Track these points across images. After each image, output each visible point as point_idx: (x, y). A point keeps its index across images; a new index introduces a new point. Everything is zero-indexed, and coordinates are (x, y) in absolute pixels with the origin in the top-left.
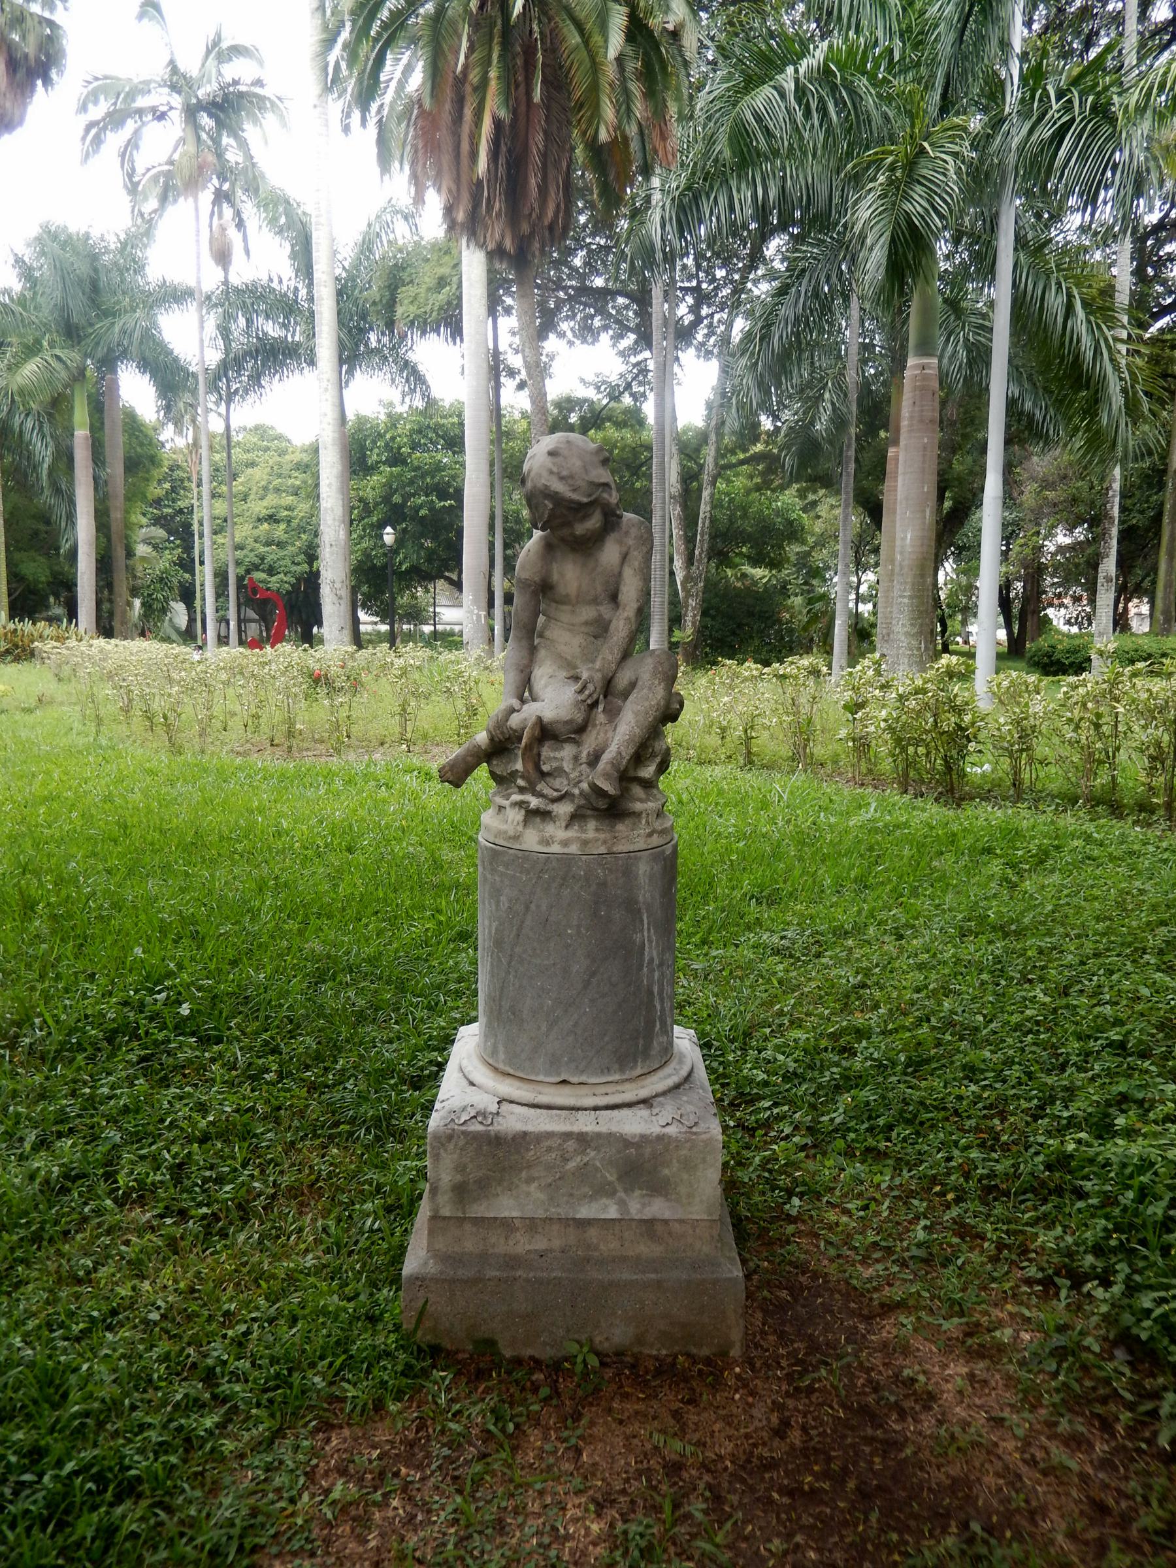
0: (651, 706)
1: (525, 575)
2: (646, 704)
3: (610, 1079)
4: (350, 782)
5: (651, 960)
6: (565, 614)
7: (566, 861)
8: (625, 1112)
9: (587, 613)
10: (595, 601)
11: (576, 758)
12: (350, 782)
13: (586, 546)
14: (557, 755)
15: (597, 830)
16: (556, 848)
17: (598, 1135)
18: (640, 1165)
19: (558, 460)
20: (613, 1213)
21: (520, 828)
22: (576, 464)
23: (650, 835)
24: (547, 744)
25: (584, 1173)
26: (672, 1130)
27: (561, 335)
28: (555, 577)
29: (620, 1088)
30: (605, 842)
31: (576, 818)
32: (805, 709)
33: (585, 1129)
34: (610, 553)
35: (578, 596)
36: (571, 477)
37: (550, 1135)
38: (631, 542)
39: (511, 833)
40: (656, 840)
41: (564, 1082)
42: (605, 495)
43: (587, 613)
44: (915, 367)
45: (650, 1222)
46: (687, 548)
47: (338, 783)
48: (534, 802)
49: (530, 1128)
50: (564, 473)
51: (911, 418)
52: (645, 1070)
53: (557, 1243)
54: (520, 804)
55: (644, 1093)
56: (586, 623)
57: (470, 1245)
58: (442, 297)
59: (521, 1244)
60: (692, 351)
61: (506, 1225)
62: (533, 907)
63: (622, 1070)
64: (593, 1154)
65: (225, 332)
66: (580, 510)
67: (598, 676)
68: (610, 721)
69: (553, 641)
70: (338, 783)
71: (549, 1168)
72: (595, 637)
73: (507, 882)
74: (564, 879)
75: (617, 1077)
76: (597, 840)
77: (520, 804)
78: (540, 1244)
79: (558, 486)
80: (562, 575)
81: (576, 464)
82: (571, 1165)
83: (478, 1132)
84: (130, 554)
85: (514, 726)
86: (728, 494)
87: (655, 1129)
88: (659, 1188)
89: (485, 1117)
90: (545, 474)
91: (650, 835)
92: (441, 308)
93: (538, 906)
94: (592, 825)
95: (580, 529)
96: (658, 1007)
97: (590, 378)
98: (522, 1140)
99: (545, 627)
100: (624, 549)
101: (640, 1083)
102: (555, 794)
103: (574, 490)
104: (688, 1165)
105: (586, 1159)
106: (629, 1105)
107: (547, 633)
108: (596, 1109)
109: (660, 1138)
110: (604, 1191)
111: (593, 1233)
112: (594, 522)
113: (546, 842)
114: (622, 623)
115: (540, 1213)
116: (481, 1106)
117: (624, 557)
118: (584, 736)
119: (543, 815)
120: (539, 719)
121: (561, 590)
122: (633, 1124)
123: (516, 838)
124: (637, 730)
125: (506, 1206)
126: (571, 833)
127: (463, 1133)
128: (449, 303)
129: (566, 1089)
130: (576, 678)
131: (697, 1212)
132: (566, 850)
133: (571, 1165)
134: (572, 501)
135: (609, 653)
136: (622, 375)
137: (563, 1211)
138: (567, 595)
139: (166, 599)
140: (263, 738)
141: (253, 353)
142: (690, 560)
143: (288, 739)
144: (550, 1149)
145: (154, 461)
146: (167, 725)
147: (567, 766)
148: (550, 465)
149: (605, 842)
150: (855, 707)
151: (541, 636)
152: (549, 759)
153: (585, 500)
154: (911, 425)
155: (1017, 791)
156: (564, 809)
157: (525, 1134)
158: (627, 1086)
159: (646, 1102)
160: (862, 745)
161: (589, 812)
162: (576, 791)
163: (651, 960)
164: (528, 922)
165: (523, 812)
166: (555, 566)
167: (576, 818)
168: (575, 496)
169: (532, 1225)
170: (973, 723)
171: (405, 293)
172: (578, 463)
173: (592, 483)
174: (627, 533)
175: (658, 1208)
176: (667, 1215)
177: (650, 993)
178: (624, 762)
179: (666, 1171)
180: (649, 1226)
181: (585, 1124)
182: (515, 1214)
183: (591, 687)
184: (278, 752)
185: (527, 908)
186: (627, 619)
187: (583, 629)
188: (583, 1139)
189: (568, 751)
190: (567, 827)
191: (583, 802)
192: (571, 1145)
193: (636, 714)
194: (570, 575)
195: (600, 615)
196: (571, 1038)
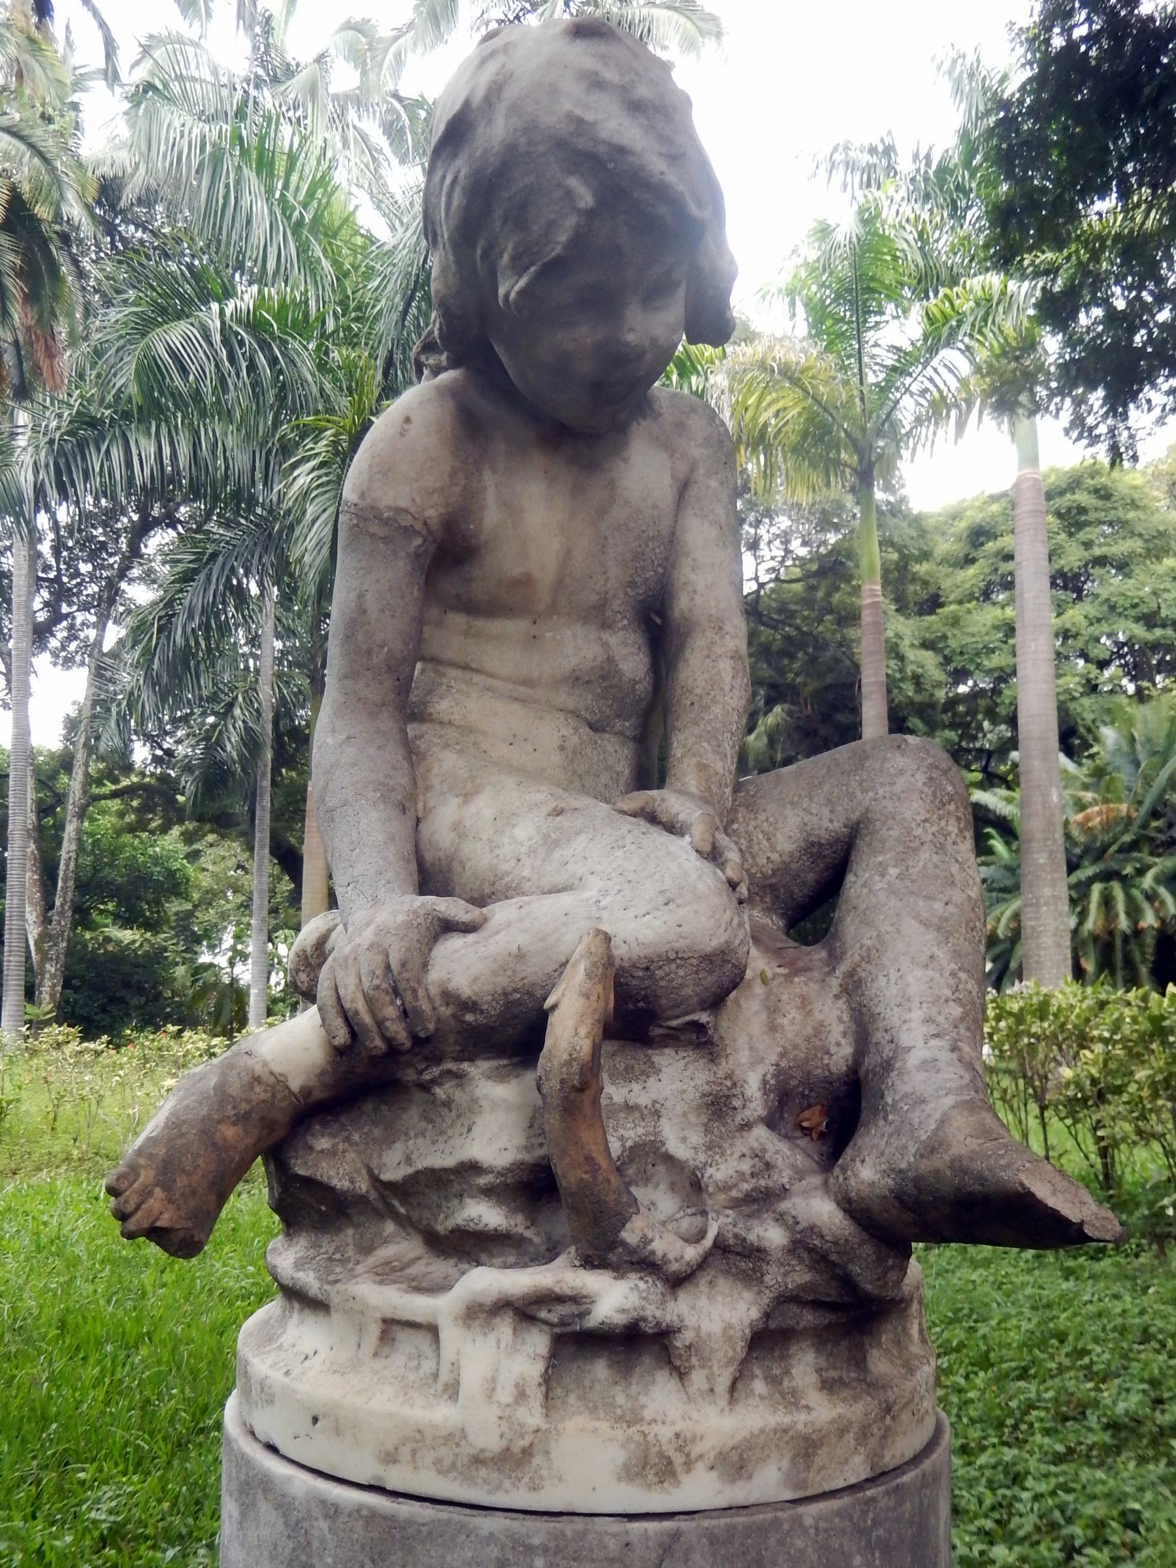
1: (395, 496)
28: (491, 516)
48: (613, 1298)
77: (524, 1311)
80: (512, 509)
85: (463, 985)
94: (804, 1367)
119: (638, 1344)
126: (756, 1416)
132: (740, 1493)
156: (719, 1314)
162: (773, 1236)
191: (800, 1276)
194: (532, 518)
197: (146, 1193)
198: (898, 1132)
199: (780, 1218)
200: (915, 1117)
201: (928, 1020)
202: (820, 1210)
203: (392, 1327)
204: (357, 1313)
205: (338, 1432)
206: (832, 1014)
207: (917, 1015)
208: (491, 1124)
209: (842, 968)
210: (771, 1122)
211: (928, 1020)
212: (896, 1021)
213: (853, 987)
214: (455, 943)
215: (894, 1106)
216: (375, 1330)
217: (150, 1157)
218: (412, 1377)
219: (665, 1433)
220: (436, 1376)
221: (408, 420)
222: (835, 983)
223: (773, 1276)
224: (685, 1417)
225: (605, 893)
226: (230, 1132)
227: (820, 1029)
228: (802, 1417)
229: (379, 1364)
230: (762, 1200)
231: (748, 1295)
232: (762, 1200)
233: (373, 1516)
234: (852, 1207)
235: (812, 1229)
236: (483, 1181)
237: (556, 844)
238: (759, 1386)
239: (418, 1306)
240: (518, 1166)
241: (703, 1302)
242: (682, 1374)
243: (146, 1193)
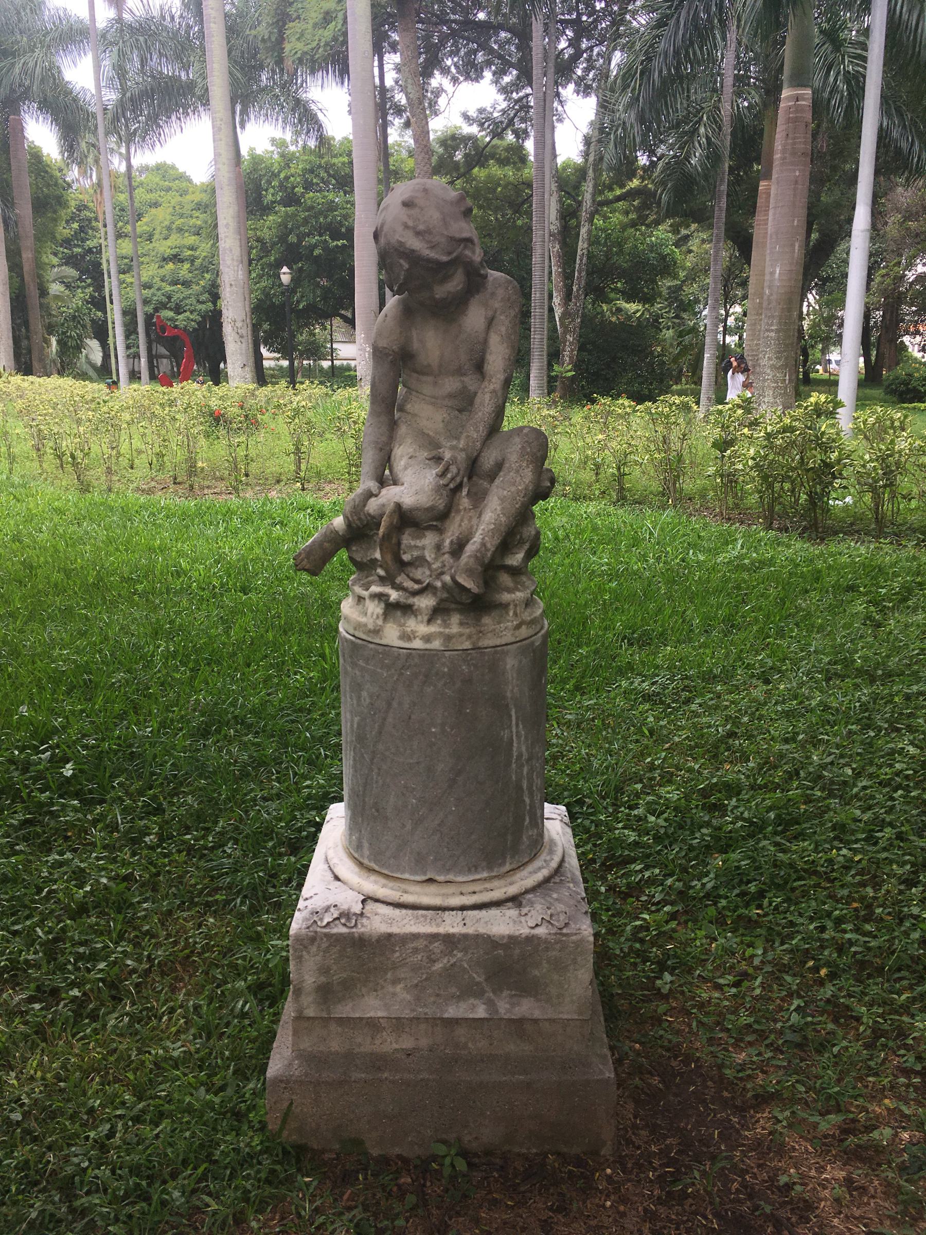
0: (518, 491)
2: (513, 489)
3: (477, 877)
4: (247, 520)
5: (520, 756)
7: (427, 656)
8: (494, 912)
9: (450, 385)
10: (459, 372)
11: (438, 547)
12: (247, 520)
13: (448, 311)
14: (419, 543)
15: (461, 624)
16: (417, 644)
17: (465, 936)
18: (508, 965)
19: (414, 212)
20: (481, 1012)
21: (380, 622)
22: (433, 216)
23: (518, 627)
24: (408, 531)
25: (450, 974)
26: (541, 931)
27: (445, 71)
28: (416, 345)
29: (488, 885)
30: (469, 637)
31: (437, 612)
32: (675, 445)
33: (452, 931)
34: (474, 318)
35: (440, 366)
36: (428, 231)
37: (416, 936)
38: (497, 305)
40: (524, 632)
41: (431, 881)
42: (468, 253)
43: (450, 385)
44: (789, 98)
45: (521, 1021)
46: (565, 285)
47: (236, 522)
48: (394, 595)
49: (395, 930)
50: (421, 227)
51: (784, 151)
52: (514, 866)
53: (424, 1042)
54: (379, 597)
55: (512, 890)
56: (451, 396)
57: (335, 1045)
58: (327, 34)
59: (389, 1044)
60: (571, 87)
61: (373, 1025)
62: (395, 704)
63: (490, 868)
64: (459, 955)
65: (120, 71)
66: (440, 270)
67: (461, 456)
68: (475, 507)
70: (236, 522)
71: (416, 969)
72: (460, 411)
73: (367, 677)
74: (426, 676)
75: (485, 875)
76: (461, 635)
77: (379, 597)
78: (407, 1043)
79: (415, 244)
81: (433, 216)
82: (438, 966)
83: (341, 934)
84: (43, 292)
85: (371, 512)
86: (604, 230)
87: (525, 931)
88: (527, 987)
89: (349, 919)
90: (400, 229)
91: (518, 627)
92: (327, 44)
93: (400, 704)
94: (455, 619)
95: (443, 290)
96: (527, 800)
97: (473, 113)
98: (388, 942)
99: (406, 400)
100: (490, 313)
101: (509, 880)
102: (416, 587)
103: (432, 248)
104: (559, 966)
105: (453, 960)
106: (497, 904)
107: (408, 407)
108: (463, 908)
109: (530, 939)
110: (470, 991)
111: (461, 1032)
112: (456, 284)
114: (487, 396)
115: (407, 1014)
116: (345, 907)
117: (490, 322)
118: (448, 523)
120: (398, 506)
122: (501, 924)
123: (377, 631)
124: (503, 519)
125: (372, 1007)
126: (433, 629)
127: (326, 935)
128: (335, 39)
129: (432, 888)
130: (438, 459)
131: (568, 1012)
132: (428, 646)
133: (438, 966)
134: (429, 260)
135: (475, 432)
136: (504, 112)
137: (430, 1011)
138: (429, 366)
139: (80, 337)
140: (166, 476)
141: (147, 94)
142: (568, 296)
143: (189, 477)
144: (416, 951)
145: (61, 202)
146: (75, 464)
147: (429, 556)
148: (405, 218)
149: (469, 637)
150: (723, 445)
151: (401, 409)
152: (411, 547)
153: (445, 258)
154: (784, 158)
155: (879, 526)
156: (425, 603)
157: (390, 936)
158: (496, 883)
159: (515, 900)
160: (730, 480)
161: (453, 606)
162: (439, 584)
163: (520, 756)
164: (390, 720)
165: (383, 605)
167: (437, 612)
168: (433, 255)
169: (398, 1025)
170: (839, 461)
171: (293, 28)
172: (436, 215)
173: (452, 239)
174: (493, 294)
175: (527, 1008)
176: (537, 1014)
177: (519, 788)
178: (489, 554)
179: (537, 973)
180: (519, 1026)
181: (451, 925)
182: (380, 1014)
183: (453, 469)
184: (181, 490)
185: (389, 704)
186: (494, 391)
188: (449, 940)
189: (429, 540)
190: (429, 621)
191: (445, 595)
192: (437, 946)
193: (502, 500)
194: (431, 343)
195: (465, 387)
196: (436, 837)
197: (302, 560)
219: (409, 629)
223: (439, 594)
226: (327, 545)
228: (447, 631)
233: (352, 642)
238: (439, 622)
242: (416, 616)
243: (302, 560)
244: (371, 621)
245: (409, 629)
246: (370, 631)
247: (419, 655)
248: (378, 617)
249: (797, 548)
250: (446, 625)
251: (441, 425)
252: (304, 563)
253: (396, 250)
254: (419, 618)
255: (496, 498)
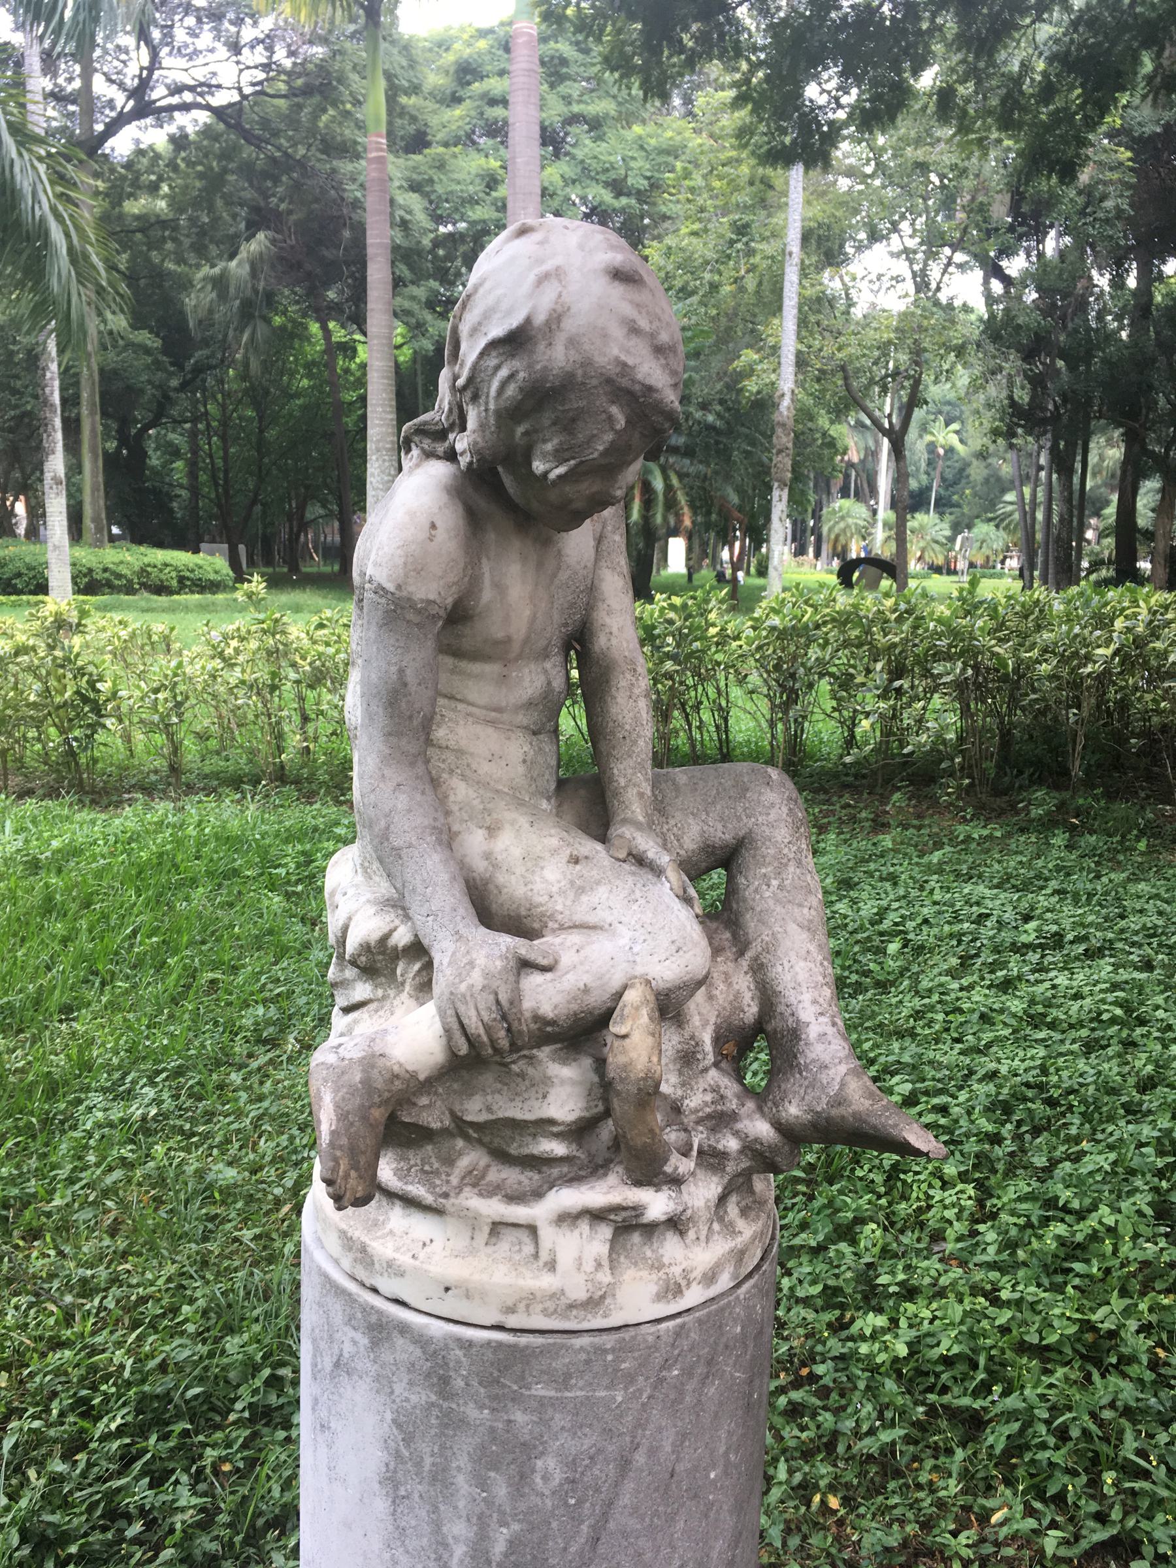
6: (479, 685)
16: (694, 1296)
35: (527, 640)
39: (579, 1293)
54: (597, 1216)
56: (530, 704)
69: (459, 752)
72: (535, 733)
80: (500, 588)
90: (617, 332)
93: (653, 1452)
113: (673, 1290)
121: (493, 627)
126: (720, 1247)
138: (508, 640)
148: (628, 311)
155: (175, 780)
156: (703, 1191)
162: (732, 1144)
165: (606, 1231)
166: (486, 567)
185: (625, 1464)
187: (522, 719)
193: (808, 928)
197: (347, 1176)
198: (812, 1086)
199: (736, 1134)
200: (824, 1078)
201: (815, 1002)
202: (762, 1129)
203: (497, 1228)
204: (471, 1221)
205: (468, 1296)
206: (743, 983)
207: (807, 997)
208: (562, 1094)
209: (749, 954)
210: (716, 1064)
211: (815, 1002)
212: (792, 1000)
213: (758, 969)
214: (533, 980)
215: (806, 1066)
216: (487, 1229)
217: (341, 1147)
218: (517, 1257)
220: (536, 1256)
221: (433, 526)
222: (745, 963)
223: (731, 1168)
224: (686, 1258)
225: (634, 941)
227: (738, 995)
228: (739, 1239)
229: (490, 1249)
230: (721, 1120)
231: (715, 1179)
232: (721, 1120)
234: (779, 1126)
235: (756, 1140)
236: (555, 1129)
237: (581, 890)
239: (520, 1213)
240: (580, 1119)
241: (692, 1188)
242: (682, 1233)
243: (347, 1176)
244: (580, 1279)
245: (676, 1271)
246: (571, 1306)
247: (700, 1321)
248: (599, 1265)
249: (84, 826)
250: (730, 1230)
251: (521, 769)
252: (352, 1182)
253: (609, 381)
254: (691, 1234)
255: (792, 928)
